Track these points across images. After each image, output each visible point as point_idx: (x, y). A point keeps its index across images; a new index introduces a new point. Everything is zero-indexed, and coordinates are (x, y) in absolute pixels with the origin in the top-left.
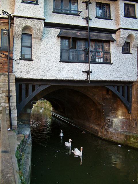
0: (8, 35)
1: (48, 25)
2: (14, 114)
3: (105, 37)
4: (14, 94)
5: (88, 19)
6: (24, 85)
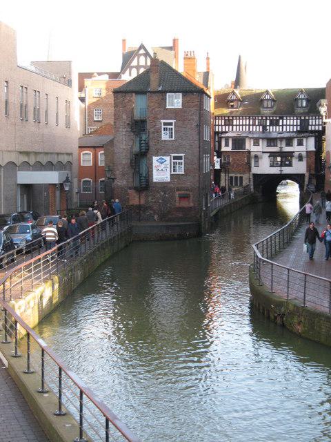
0: (249, 158)
1: (263, 152)
2: (252, 187)
3: (291, 154)
4: (252, 180)
5: (281, 148)
6: (255, 175)
